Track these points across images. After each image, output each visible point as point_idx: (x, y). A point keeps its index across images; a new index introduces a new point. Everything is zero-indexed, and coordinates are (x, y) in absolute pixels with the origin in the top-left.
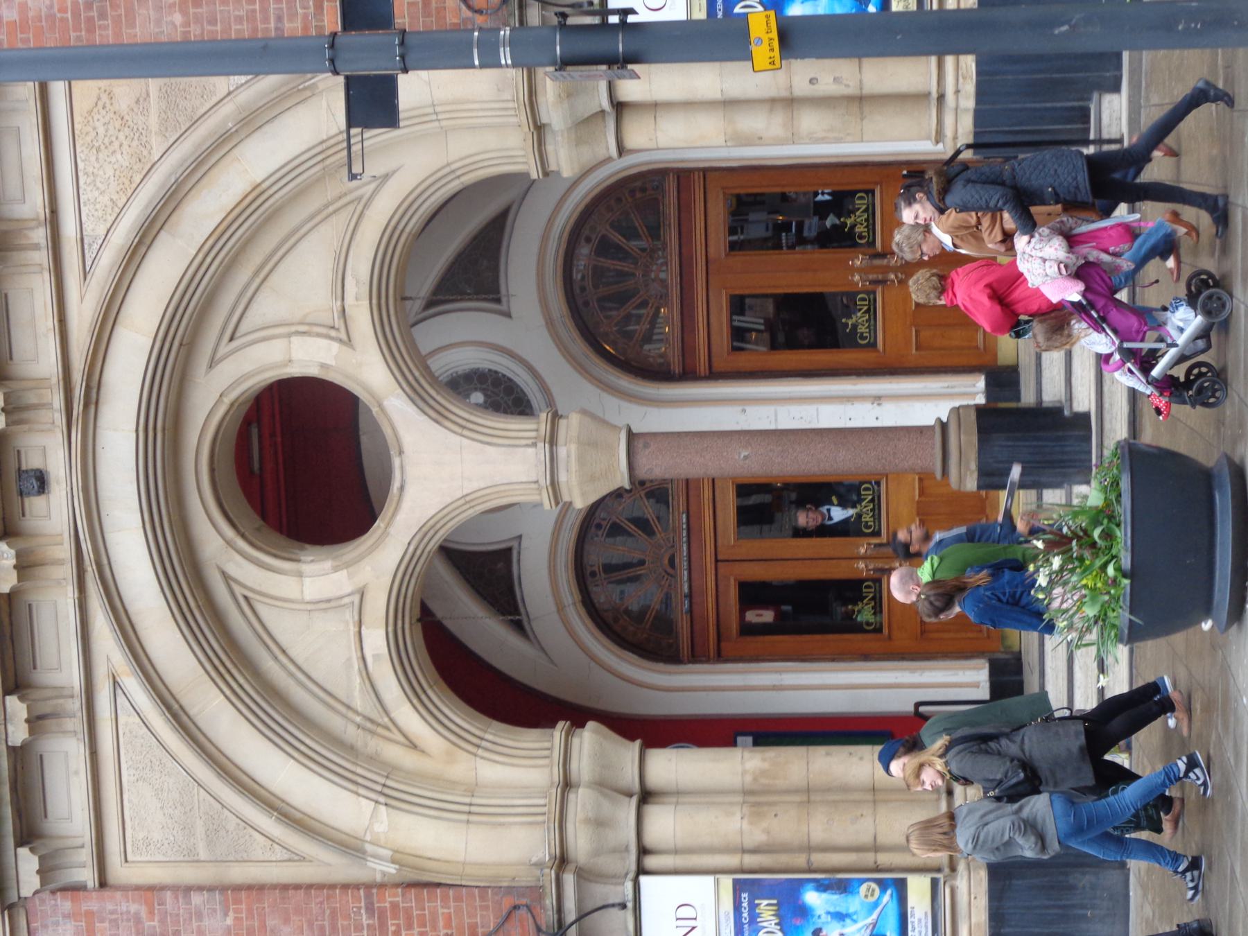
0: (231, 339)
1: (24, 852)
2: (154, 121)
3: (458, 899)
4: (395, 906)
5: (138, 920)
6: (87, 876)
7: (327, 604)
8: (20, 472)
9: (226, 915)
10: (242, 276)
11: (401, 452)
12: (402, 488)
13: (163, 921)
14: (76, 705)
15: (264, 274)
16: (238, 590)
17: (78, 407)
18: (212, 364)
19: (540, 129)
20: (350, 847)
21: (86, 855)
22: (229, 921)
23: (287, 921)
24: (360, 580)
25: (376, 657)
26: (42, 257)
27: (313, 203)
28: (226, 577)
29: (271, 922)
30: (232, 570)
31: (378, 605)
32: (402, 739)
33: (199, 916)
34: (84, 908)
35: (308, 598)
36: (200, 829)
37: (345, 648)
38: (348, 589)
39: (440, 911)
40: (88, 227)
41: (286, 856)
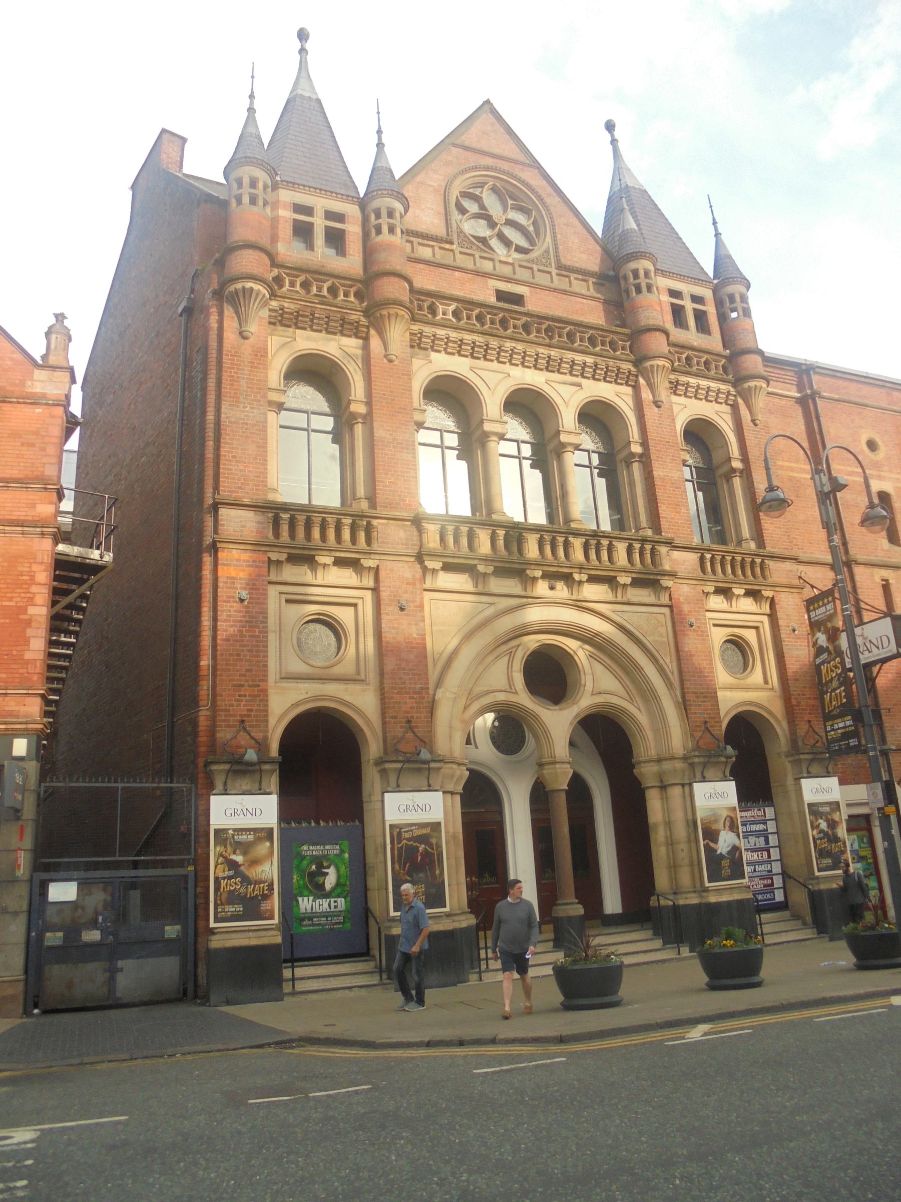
0: (590, 656)
1: (441, 564)
2: (657, 638)
3: (427, 722)
4: (424, 698)
5: (414, 601)
6: (428, 585)
9: (417, 634)
12: (549, 709)
17: (579, 604)
19: (659, 761)
22: (415, 636)
24: (519, 692)
26: (619, 599)
30: (520, 648)
31: (513, 698)
32: (468, 704)
33: (416, 625)
35: (513, 674)
38: (517, 688)
39: (423, 715)
41: (436, 659)
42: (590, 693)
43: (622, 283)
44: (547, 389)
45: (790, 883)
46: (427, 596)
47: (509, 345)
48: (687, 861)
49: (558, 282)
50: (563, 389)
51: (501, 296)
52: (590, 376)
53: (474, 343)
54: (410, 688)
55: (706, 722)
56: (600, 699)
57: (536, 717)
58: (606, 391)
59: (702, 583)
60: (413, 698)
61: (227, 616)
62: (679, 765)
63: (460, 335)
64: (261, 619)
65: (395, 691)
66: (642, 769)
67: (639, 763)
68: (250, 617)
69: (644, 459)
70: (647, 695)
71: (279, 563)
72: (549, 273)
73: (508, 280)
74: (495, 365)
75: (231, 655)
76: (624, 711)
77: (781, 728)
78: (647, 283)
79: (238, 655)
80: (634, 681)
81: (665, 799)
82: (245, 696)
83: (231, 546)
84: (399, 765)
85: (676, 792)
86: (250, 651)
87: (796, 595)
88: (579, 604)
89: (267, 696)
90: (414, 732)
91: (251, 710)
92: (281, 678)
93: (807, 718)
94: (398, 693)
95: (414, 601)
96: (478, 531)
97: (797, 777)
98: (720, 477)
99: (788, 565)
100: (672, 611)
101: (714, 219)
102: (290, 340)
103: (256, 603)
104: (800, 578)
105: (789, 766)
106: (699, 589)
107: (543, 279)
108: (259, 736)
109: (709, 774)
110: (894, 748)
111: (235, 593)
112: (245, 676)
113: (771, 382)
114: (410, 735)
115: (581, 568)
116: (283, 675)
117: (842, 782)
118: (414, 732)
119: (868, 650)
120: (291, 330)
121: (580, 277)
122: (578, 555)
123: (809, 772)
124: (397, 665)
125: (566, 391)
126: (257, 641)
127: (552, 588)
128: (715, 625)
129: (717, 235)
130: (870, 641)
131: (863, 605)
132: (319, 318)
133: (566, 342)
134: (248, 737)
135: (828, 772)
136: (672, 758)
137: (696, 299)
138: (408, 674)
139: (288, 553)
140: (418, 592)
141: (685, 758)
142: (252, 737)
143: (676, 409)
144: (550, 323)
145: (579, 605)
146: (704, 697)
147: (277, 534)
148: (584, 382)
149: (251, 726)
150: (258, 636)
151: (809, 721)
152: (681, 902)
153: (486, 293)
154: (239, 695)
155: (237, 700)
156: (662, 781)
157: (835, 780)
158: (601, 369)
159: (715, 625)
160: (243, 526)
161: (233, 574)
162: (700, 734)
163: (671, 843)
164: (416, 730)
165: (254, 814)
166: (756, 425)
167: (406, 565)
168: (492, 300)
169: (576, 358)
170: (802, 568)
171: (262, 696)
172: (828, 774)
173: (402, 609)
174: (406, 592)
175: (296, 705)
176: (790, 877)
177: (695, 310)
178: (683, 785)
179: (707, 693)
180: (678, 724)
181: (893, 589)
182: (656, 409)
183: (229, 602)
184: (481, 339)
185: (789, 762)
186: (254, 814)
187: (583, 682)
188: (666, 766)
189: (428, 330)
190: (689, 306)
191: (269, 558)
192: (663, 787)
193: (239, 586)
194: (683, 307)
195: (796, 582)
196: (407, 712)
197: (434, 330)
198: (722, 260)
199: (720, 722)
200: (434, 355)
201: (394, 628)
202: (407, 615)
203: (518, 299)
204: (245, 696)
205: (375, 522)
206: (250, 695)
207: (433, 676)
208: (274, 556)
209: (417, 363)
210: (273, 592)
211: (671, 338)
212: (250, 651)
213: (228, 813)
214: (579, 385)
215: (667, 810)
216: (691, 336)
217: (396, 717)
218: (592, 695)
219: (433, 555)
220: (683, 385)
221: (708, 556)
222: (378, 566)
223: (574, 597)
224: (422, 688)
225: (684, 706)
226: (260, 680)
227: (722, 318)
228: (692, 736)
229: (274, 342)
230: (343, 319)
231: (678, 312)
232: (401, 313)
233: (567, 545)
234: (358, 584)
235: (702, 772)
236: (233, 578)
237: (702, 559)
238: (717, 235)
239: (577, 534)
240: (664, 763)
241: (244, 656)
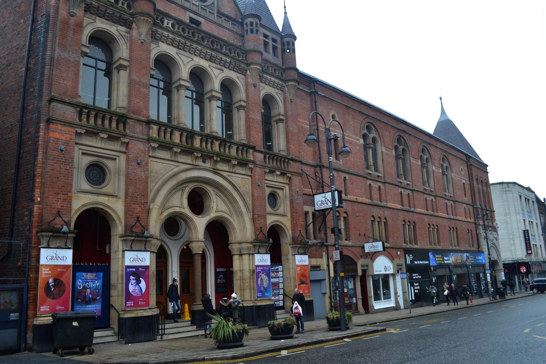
3: (146, 218)
4: (145, 207)
5: (144, 161)
6: (151, 154)
7: (182, 203)
8: (206, 159)
10: (224, 197)
11: (202, 217)
12: (197, 217)
13: (143, 165)
14: (176, 159)
15: (223, 200)
16: (184, 188)
17: (215, 171)
18: (213, 190)
19: (240, 243)
20: (153, 200)
21: (154, 155)
22: (143, 177)
23: (143, 187)
25: (175, 209)
26: (231, 170)
27: (232, 209)
28: (186, 187)
29: (143, 184)
30: (187, 188)
31: (182, 210)
33: (144, 172)
34: (146, 152)
36: (155, 175)
37: (175, 204)
38: (184, 206)
40: (234, 177)
42: (215, 211)
43: (245, 26)
44: (208, 69)
45: (286, 298)
47: (195, 46)
48: (248, 287)
49: (216, 19)
50: (215, 70)
51: (192, 20)
52: (227, 67)
53: (180, 41)
54: (140, 202)
55: (261, 228)
56: (219, 214)
57: (191, 220)
58: (233, 75)
59: (265, 167)
60: (141, 207)
61: (53, 158)
63: (174, 36)
64: (71, 161)
65: (133, 203)
66: (233, 246)
68: (65, 159)
69: (246, 109)
70: (240, 214)
71: (80, 134)
72: (213, 14)
73: (196, 13)
74: (187, 54)
75: (55, 178)
76: (228, 220)
77: (289, 233)
78: (256, 29)
79: (58, 178)
80: (234, 207)
81: (241, 260)
82: (60, 199)
83: (58, 122)
84: (133, 238)
85: (246, 257)
86: (64, 177)
87: (300, 177)
88: (215, 171)
89: (71, 200)
90: (140, 223)
91: (63, 206)
92: (78, 192)
93: (299, 229)
94: (134, 204)
95: (144, 161)
96: (175, 132)
97: (293, 254)
98: (274, 121)
99: (298, 164)
100: (252, 178)
101: (285, 6)
102: (93, 21)
103: (69, 153)
104: (302, 170)
105: (290, 249)
106: (263, 170)
107: (211, 17)
108: (66, 219)
109: (261, 250)
110: (330, 244)
111: (58, 146)
112: (61, 189)
113: (300, 84)
114: (138, 224)
115: (236, 159)
116: (79, 190)
117: (310, 257)
118: (140, 223)
119: (326, 203)
120: (94, 16)
121: (226, 19)
122: (216, 148)
123: (298, 252)
124: (134, 190)
125: (217, 72)
126: (68, 172)
127: (204, 162)
128: (267, 186)
129: (286, 13)
131: (324, 184)
132: (109, 14)
133: (244, 60)
134: (61, 220)
135: (305, 253)
137: (274, 40)
138: (139, 195)
139: (86, 130)
140: (146, 157)
142: (63, 220)
143: (261, 88)
144: (213, 39)
145: (215, 171)
146: (261, 217)
147: (80, 120)
148: (225, 69)
149: (62, 214)
150: (69, 170)
151: (300, 231)
152: (245, 305)
153: (185, 17)
154: (57, 198)
155: (56, 201)
156: (240, 252)
158: (233, 65)
159: (267, 186)
160: (64, 113)
161: (58, 137)
162: (258, 233)
163: (242, 279)
164: (141, 222)
165: (62, 259)
166: (291, 101)
167: (141, 143)
168: (188, 21)
169: (223, 57)
170: (303, 166)
171: (69, 201)
172: (305, 254)
173: (139, 164)
174: (141, 156)
175: (84, 205)
176: (286, 296)
177: (273, 45)
178: (249, 254)
179: (262, 215)
180: (250, 228)
182: (253, 88)
183: (55, 151)
184: (183, 41)
185: (291, 247)
186: (62, 259)
187: (212, 206)
188: (244, 245)
189: (160, 31)
190: (271, 43)
191: (76, 131)
192: (241, 255)
193: (60, 143)
194: (268, 43)
195: (300, 171)
196: (137, 213)
197: (163, 31)
198: (287, 24)
199: (267, 228)
200: (160, 43)
201: (134, 173)
202: (141, 167)
203: (198, 23)
204: (60, 199)
205: (129, 121)
206: (63, 199)
207: (151, 196)
208: (79, 130)
209: (153, 46)
210: (77, 148)
211: (263, 56)
212: (64, 177)
213: (48, 258)
214: (222, 70)
215: (241, 265)
216: (269, 56)
217: (132, 215)
218: (216, 212)
219: (154, 141)
220: (265, 78)
221: (268, 156)
222: (128, 142)
223: (213, 167)
224: (145, 202)
225: (254, 220)
226: (69, 192)
227: (284, 51)
228: (255, 233)
229: (86, 20)
230: (120, 16)
231: (266, 44)
232: (150, 20)
233: (212, 143)
234: (191, 163)
235: (258, 250)
236: (57, 139)
237: (265, 157)
238: (286, 13)
239: (235, 144)
240: (243, 244)
241: (61, 179)
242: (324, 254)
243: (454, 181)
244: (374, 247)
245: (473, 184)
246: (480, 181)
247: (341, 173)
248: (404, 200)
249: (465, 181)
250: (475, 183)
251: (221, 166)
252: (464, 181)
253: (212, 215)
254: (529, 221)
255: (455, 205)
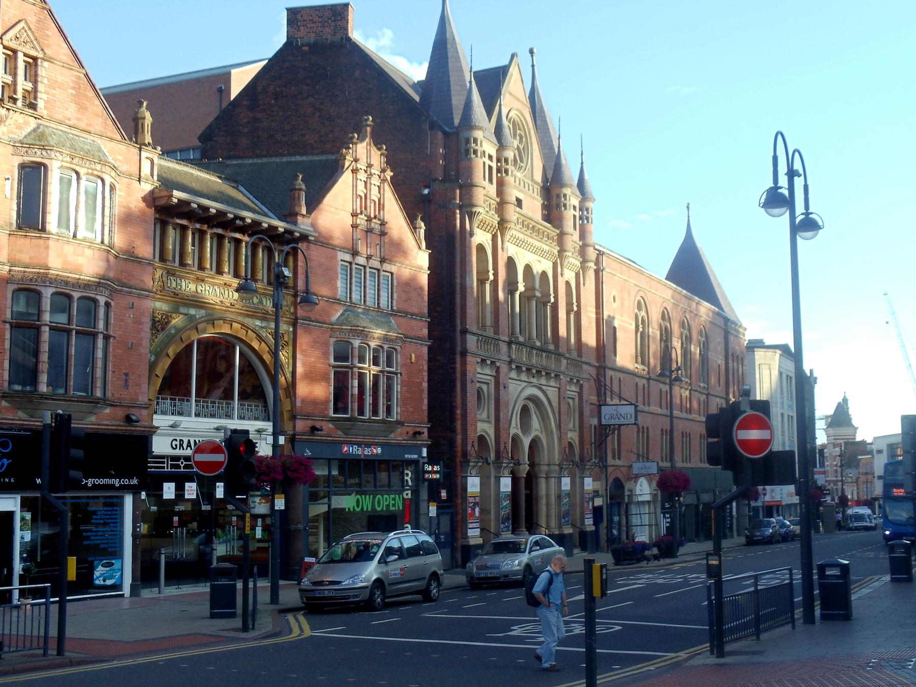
19: (549, 465)
46: (510, 381)
62: (557, 468)
67: (540, 465)
81: (547, 484)
117: (593, 481)
130: (620, 414)
136: (555, 465)
141: (559, 465)
157: (591, 479)
181: (613, 380)
188: (552, 467)
215: (548, 489)
242: (604, 476)
243: (709, 364)
244: (645, 468)
245: (728, 363)
246: (735, 358)
247: (617, 373)
248: (663, 398)
249: (721, 361)
250: (730, 362)
251: (543, 381)
252: (719, 362)
253: (533, 434)
254: (789, 416)
255: (707, 401)
